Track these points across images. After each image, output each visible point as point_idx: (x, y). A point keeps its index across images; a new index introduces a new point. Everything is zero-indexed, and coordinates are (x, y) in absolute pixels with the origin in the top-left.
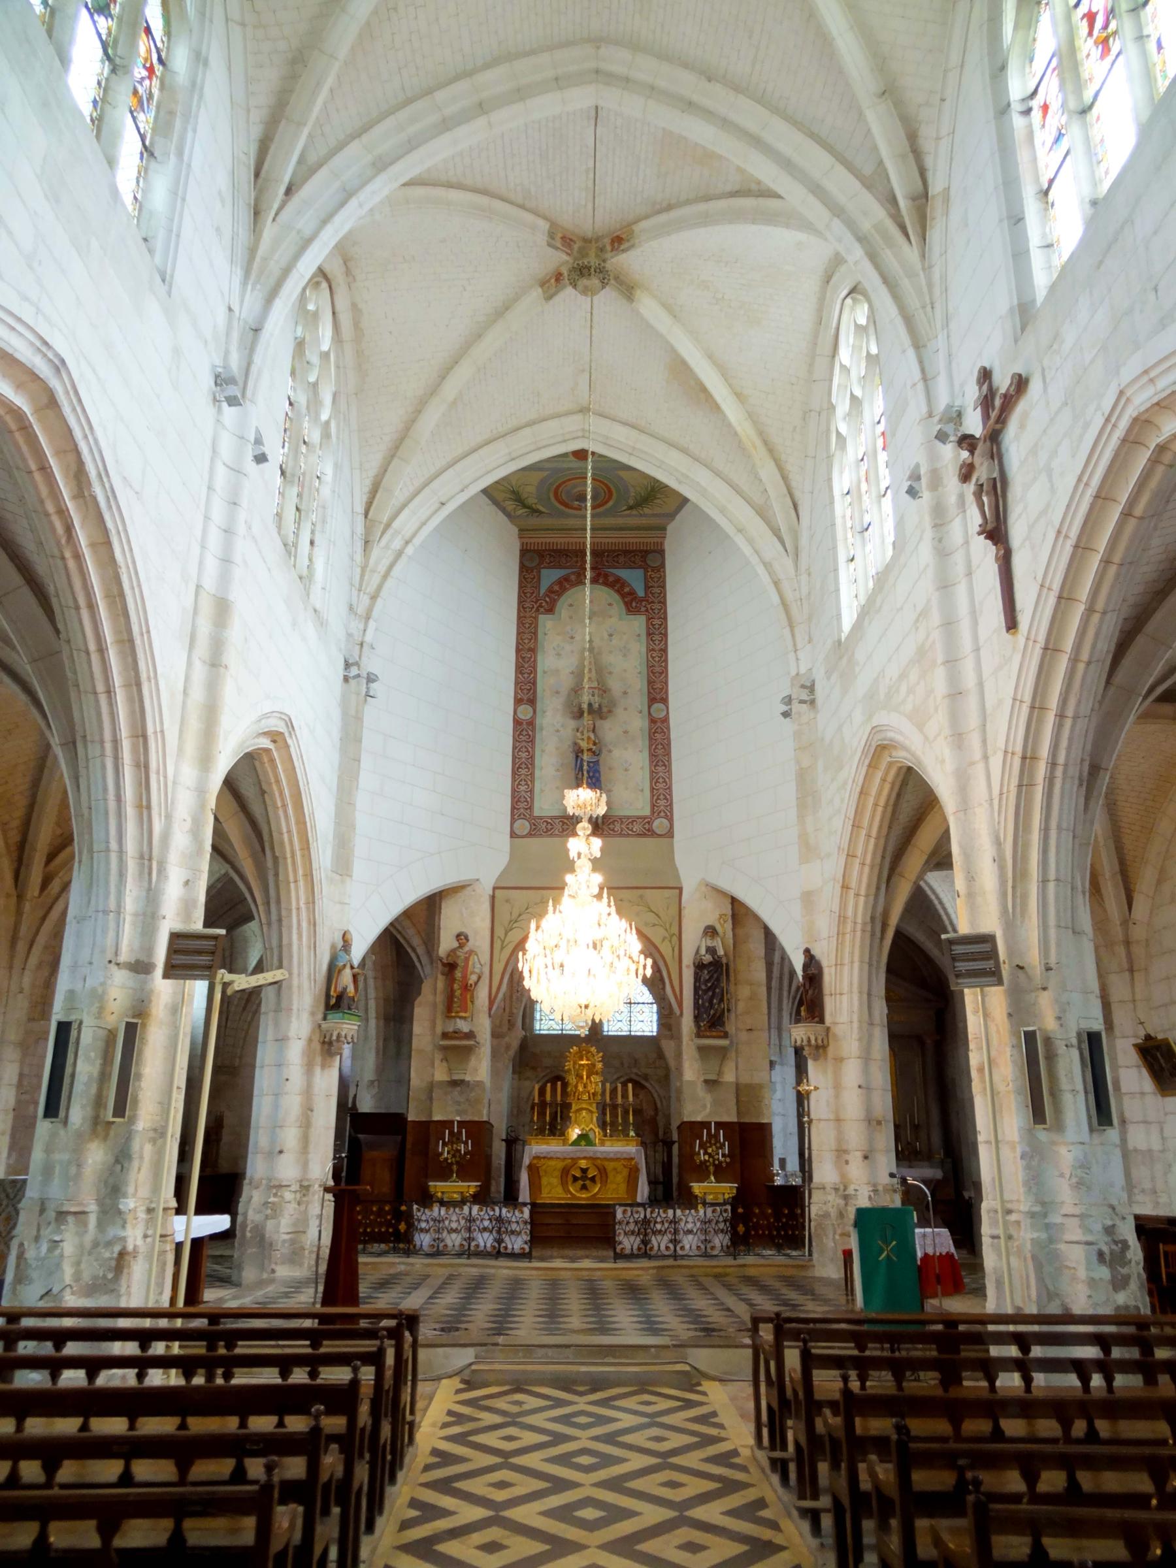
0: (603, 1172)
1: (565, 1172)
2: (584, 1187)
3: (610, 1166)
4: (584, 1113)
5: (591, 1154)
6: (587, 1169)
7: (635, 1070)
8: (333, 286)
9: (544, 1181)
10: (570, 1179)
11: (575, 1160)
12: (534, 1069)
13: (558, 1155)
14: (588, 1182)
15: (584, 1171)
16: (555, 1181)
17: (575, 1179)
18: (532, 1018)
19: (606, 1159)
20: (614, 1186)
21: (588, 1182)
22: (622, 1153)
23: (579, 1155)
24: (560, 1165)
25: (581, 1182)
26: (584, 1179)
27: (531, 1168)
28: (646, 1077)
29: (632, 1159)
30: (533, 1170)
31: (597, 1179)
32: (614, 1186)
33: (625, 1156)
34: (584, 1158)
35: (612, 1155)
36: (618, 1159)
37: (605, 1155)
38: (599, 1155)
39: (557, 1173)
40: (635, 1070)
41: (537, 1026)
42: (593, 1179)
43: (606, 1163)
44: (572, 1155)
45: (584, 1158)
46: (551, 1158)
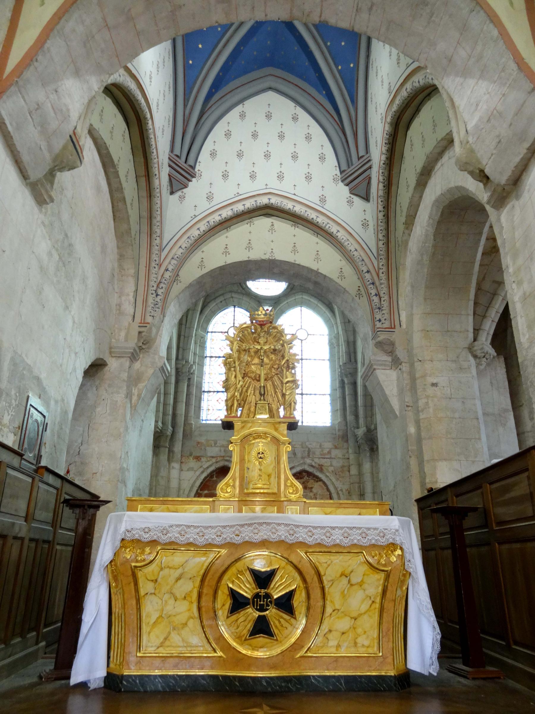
0: (314, 582)
1: (209, 581)
2: (262, 628)
3: (331, 566)
4: (260, 445)
5: (282, 534)
6: (272, 574)
7: (308, 461)
8: (129, 121)
9: (151, 608)
10: (224, 602)
11: (238, 548)
12: (198, 458)
13: (192, 536)
14: (272, 613)
15: (263, 579)
16: (184, 610)
17: (238, 603)
18: (199, 408)
19: (322, 548)
20: (344, 624)
21: (272, 613)
22: (364, 531)
23: (247, 534)
24: (199, 562)
25: (252, 613)
26: (262, 604)
27: (114, 568)
28: (321, 468)
29: (393, 546)
30: (125, 577)
31: (298, 602)
32: (344, 624)
33: (373, 538)
34: (264, 544)
35: (337, 537)
36: (355, 549)
37: (318, 537)
38: (302, 536)
39: (189, 587)
40: (308, 461)
41: (204, 415)
42: (286, 604)
43: (320, 559)
44: (229, 536)
45: (264, 544)
46: (172, 546)
